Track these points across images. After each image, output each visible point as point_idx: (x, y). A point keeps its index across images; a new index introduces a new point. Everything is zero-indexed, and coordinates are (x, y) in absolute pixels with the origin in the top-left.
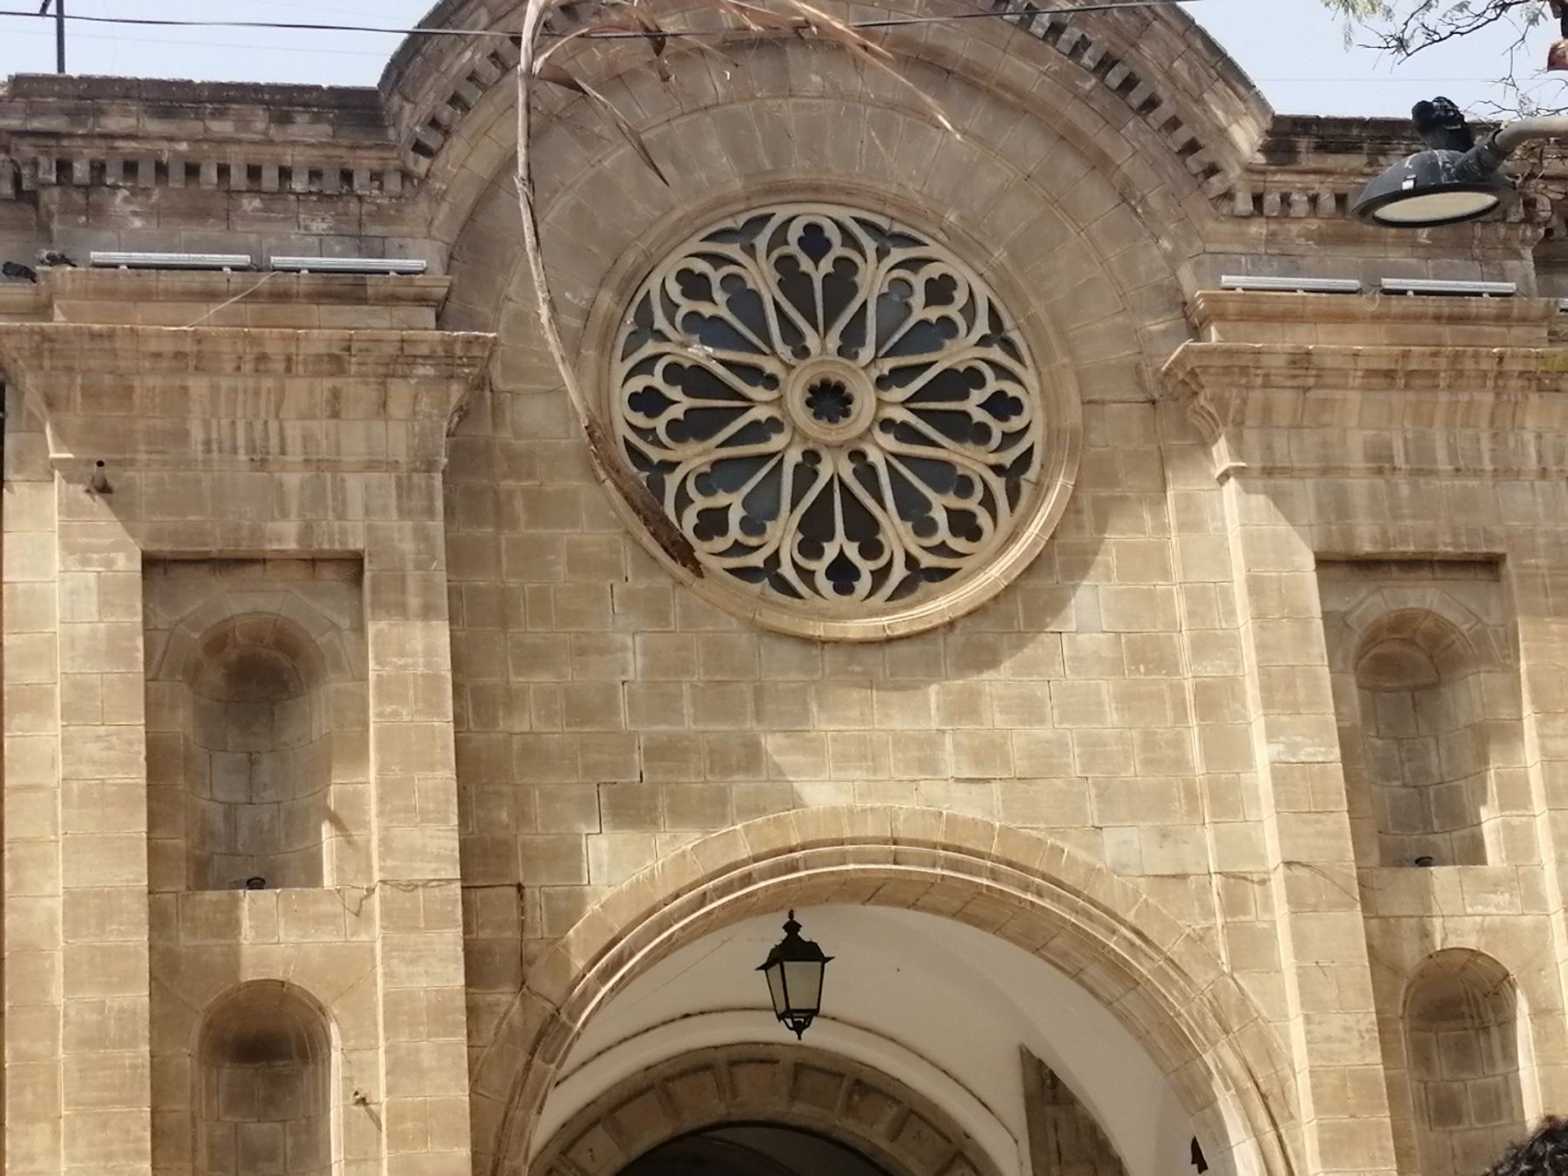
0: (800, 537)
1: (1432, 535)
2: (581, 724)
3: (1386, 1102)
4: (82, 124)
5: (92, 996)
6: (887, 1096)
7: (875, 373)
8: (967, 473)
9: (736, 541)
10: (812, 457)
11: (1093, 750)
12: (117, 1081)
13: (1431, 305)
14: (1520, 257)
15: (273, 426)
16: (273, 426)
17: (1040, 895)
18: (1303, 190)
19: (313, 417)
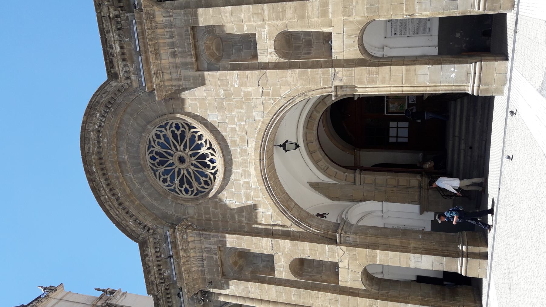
0: (207, 168)
1: (188, 44)
2: (244, 211)
3: (306, 69)
5: (292, 296)
6: (312, 113)
7: (175, 151)
8: (191, 136)
10: (192, 164)
11: (240, 119)
12: (306, 294)
13: (141, 41)
14: (127, 17)
15: (198, 257)
16: (198, 257)
17: (268, 133)
19: (196, 251)
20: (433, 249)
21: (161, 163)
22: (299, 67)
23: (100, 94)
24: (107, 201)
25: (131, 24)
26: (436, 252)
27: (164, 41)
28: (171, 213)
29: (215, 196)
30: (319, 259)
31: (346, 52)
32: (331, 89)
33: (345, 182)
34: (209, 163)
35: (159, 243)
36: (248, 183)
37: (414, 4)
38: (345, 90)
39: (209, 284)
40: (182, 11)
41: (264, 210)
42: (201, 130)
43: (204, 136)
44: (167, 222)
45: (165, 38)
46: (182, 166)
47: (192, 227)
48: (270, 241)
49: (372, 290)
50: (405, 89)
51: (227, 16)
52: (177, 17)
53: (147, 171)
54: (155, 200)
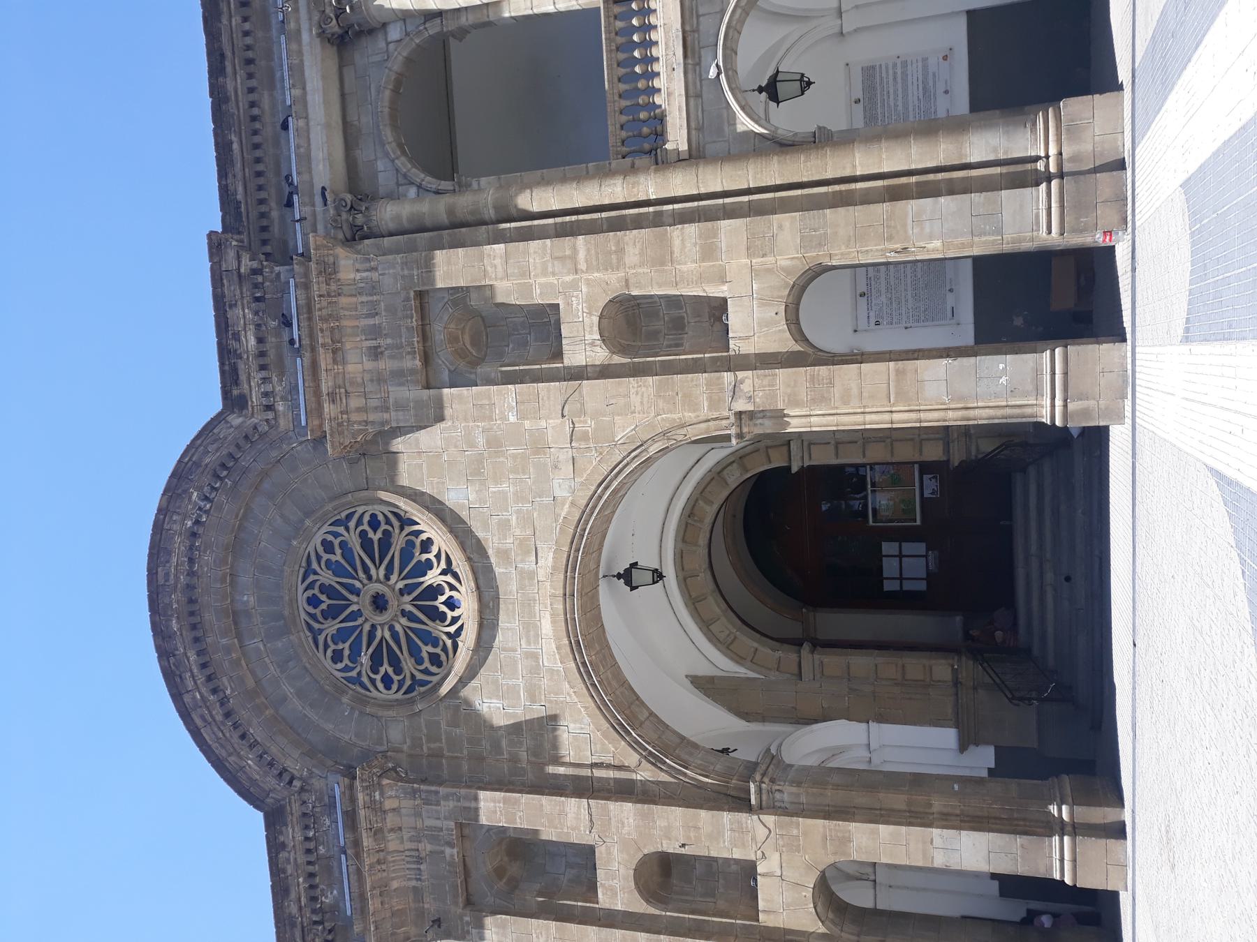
0: (438, 622)
1: (407, 328)
2: (522, 730)
4: (296, 922)
6: (694, 505)
7: (365, 581)
8: (404, 542)
9: (442, 650)
10: (403, 613)
11: (519, 498)
13: (304, 324)
15: (407, 853)
16: (407, 853)
17: (585, 530)
18: (259, 386)
19: (402, 837)
20: (988, 817)
21: (331, 613)
22: (654, 372)
23: (204, 443)
24: (196, 706)
25: (285, 290)
26: (996, 824)
27: (356, 323)
28: (347, 738)
29: (454, 692)
30: (707, 855)
31: (759, 337)
32: (728, 421)
33: (777, 673)
34: (443, 608)
35: (313, 815)
36: (534, 656)
37: (905, 226)
38: (760, 424)
39: (432, 926)
40: (399, 258)
41: (572, 726)
42: (429, 528)
43: (435, 541)
44: (336, 762)
45: (357, 318)
46: (379, 618)
47: (397, 772)
48: (586, 806)
49: (843, 934)
50: (896, 416)
51: (496, 268)
52: (387, 272)
53: (298, 632)
54: (311, 705)
